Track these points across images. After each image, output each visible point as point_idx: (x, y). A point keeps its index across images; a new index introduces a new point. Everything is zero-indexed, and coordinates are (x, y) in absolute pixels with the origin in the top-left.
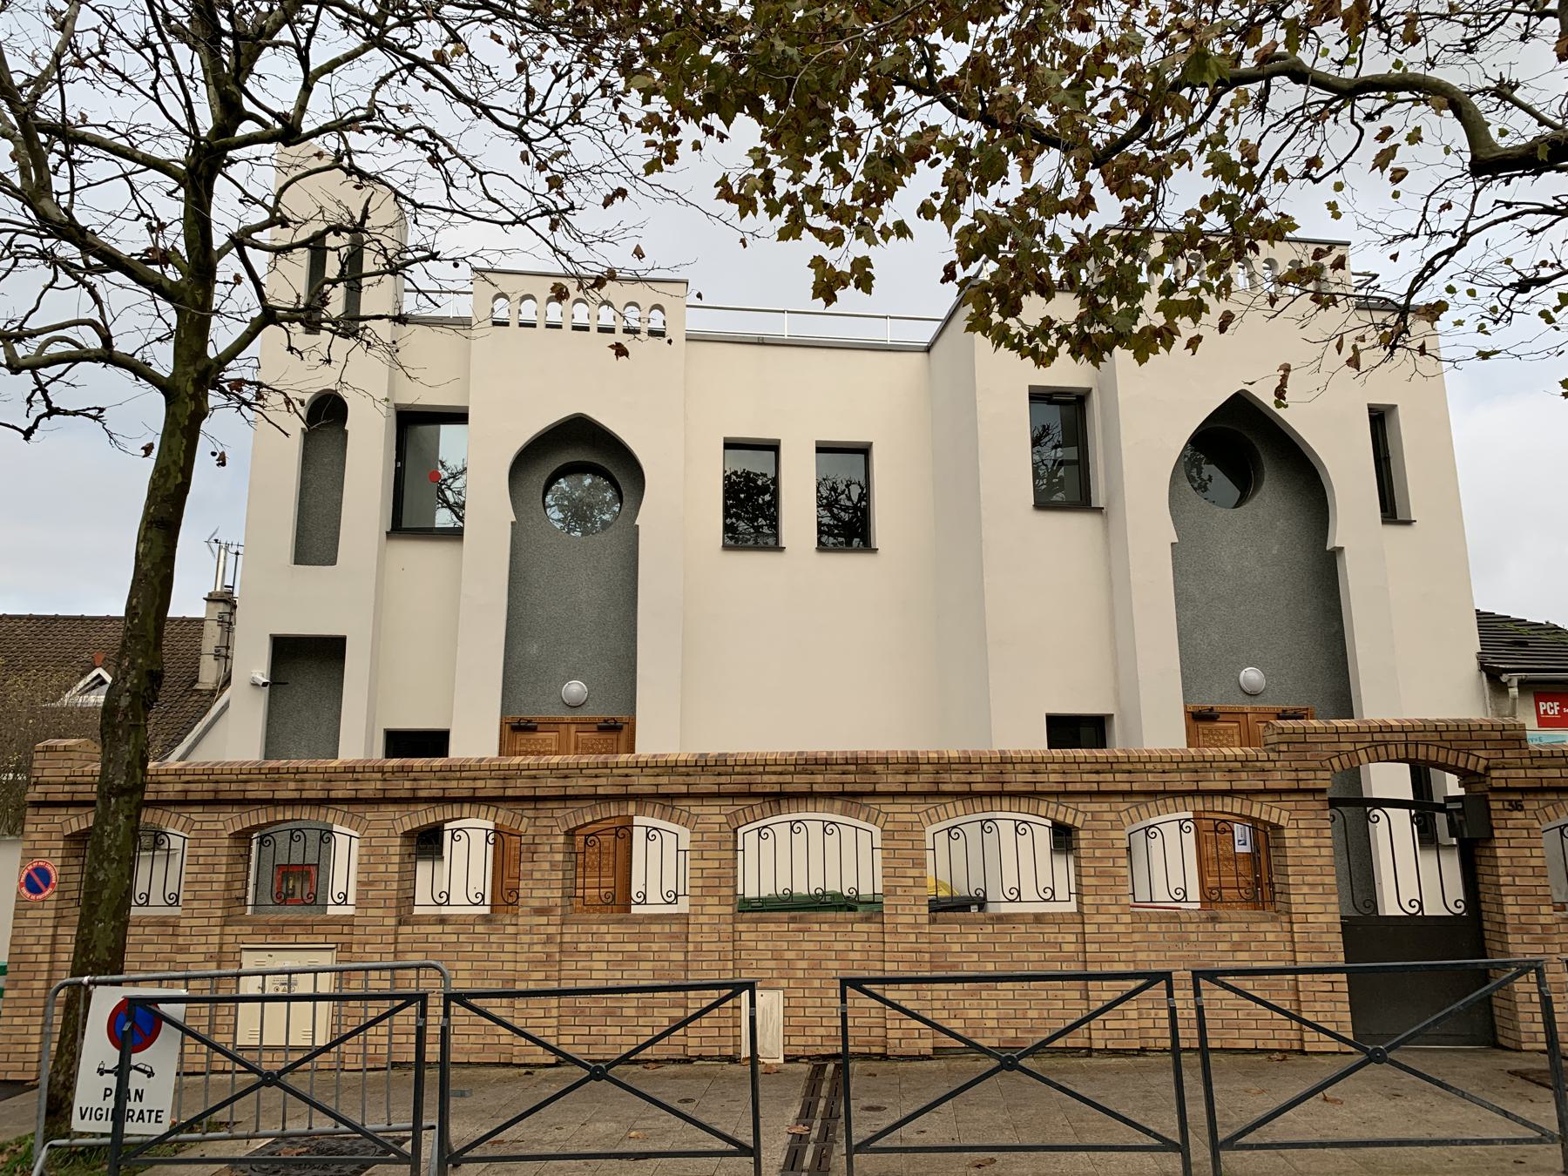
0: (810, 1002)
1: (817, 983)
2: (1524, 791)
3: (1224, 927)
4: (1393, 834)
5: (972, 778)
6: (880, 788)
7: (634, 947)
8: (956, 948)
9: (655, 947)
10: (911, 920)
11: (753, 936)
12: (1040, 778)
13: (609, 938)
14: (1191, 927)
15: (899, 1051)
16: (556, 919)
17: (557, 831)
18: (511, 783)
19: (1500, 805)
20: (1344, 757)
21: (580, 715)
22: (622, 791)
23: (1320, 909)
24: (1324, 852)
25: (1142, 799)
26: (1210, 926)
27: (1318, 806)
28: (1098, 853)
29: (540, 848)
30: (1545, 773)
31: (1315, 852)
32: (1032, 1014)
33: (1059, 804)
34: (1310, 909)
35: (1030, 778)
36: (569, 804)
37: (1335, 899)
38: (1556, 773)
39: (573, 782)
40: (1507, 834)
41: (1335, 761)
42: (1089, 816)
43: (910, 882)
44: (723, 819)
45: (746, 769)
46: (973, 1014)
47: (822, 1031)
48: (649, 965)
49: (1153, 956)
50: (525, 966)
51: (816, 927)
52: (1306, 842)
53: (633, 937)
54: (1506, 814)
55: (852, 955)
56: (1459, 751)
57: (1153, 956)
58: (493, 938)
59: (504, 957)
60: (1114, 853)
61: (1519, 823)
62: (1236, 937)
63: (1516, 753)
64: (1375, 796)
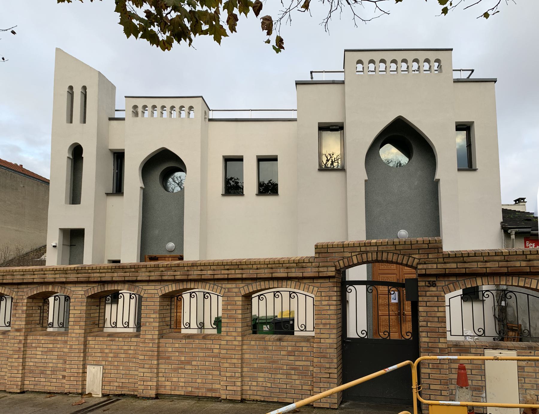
0: (113, 371)
1: (116, 363)
2: (437, 276)
3: (285, 344)
4: (358, 298)
5: (176, 273)
6: (139, 278)
7: (51, 346)
8: (170, 349)
9: (59, 346)
10: (150, 337)
11: (93, 342)
12: (204, 272)
13: (43, 341)
14: (270, 343)
15: (142, 395)
16: (22, 334)
17: (24, 297)
18: (5, 277)
19: (423, 284)
20: (346, 260)
21: (173, 254)
22: (42, 280)
23: (327, 336)
24: (332, 308)
25: (250, 282)
26: (278, 343)
27: (331, 284)
28: (229, 307)
29: (19, 304)
30: (448, 266)
31: (327, 307)
32: (199, 381)
33: (214, 284)
34: (323, 336)
35: (199, 273)
36: (29, 286)
37: (335, 331)
38: (454, 266)
39: (25, 277)
40: (426, 299)
41: (341, 262)
42: (227, 290)
43: (152, 320)
44: (83, 293)
45: (93, 271)
46: (175, 379)
47: (116, 384)
48: (56, 353)
49: (252, 356)
50: (11, 352)
51: (117, 339)
52: (324, 303)
53: (52, 342)
54: (427, 289)
55: (130, 352)
56: (404, 255)
57: (252, 356)
58: (5, 341)
59: (8, 348)
60: (236, 307)
61: (433, 293)
62: (290, 349)
63: (435, 255)
64: (350, 280)
